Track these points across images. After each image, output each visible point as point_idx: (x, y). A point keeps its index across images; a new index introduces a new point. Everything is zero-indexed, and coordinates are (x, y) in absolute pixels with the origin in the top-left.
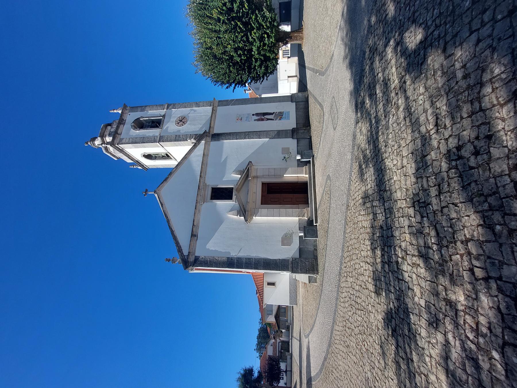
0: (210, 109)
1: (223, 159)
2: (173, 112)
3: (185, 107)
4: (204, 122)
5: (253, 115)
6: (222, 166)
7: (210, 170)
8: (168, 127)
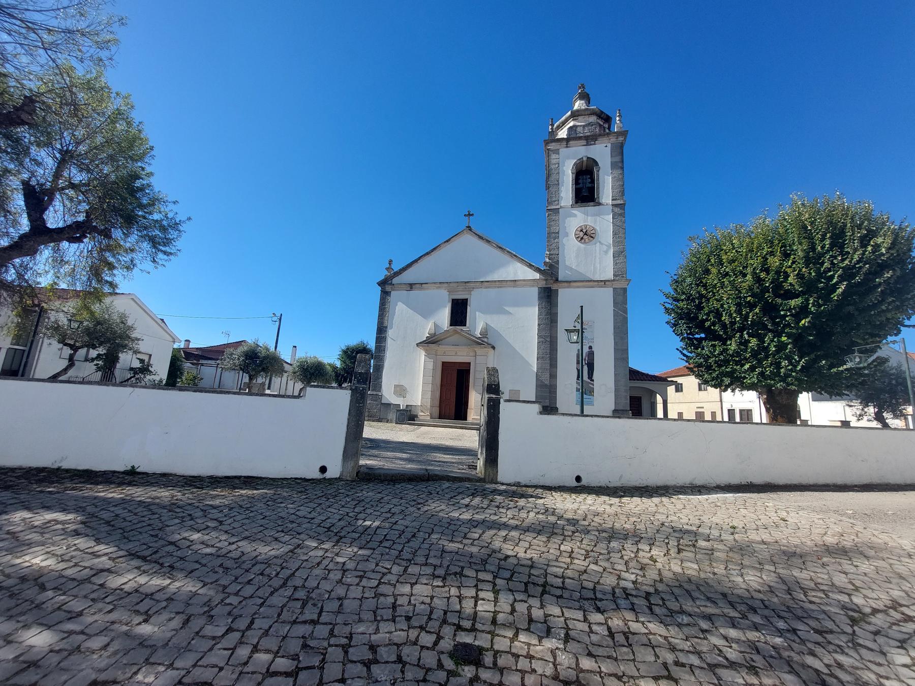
0: (609, 274)
1: (507, 309)
2: (606, 217)
3: (615, 234)
4: (582, 269)
5: (590, 347)
6: (499, 309)
7: (492, 292)
8: (575, 216)
